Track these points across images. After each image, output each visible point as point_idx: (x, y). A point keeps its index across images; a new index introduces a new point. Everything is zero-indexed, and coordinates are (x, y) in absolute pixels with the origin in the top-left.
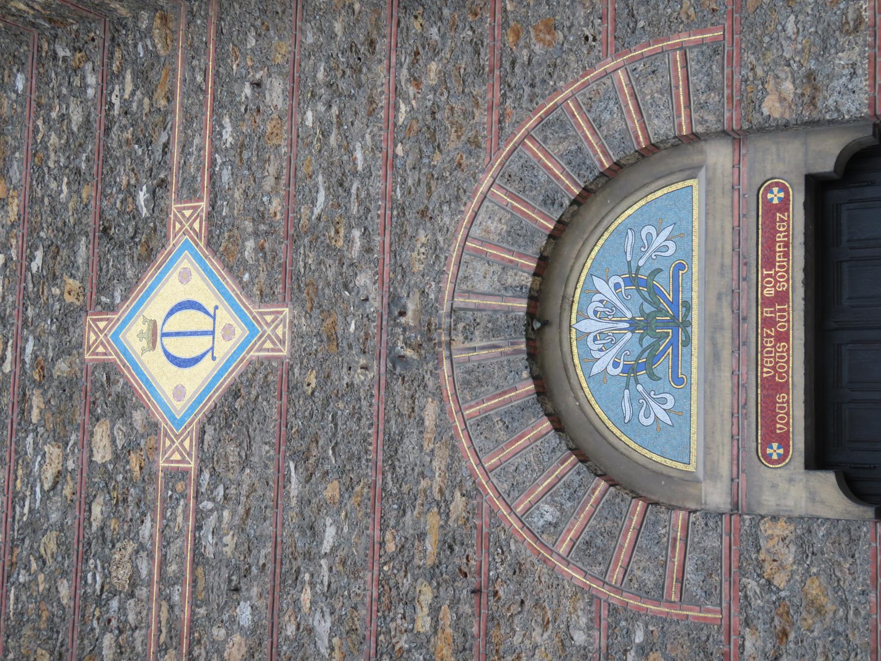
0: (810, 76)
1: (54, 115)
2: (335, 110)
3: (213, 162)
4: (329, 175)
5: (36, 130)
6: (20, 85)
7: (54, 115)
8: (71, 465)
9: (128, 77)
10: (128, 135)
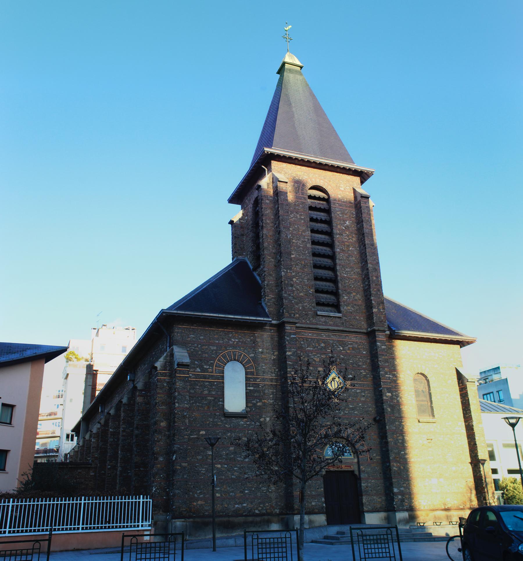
0: (365, 471)
1: (360, 360)
2: (361, 408)
3: (355, 388)
4: (354, 407)
5: (358, 356)
6: (364, 352)
7: (360, 360)
8: (317, 363)
9: (365, 373)
10: (358, 374)
